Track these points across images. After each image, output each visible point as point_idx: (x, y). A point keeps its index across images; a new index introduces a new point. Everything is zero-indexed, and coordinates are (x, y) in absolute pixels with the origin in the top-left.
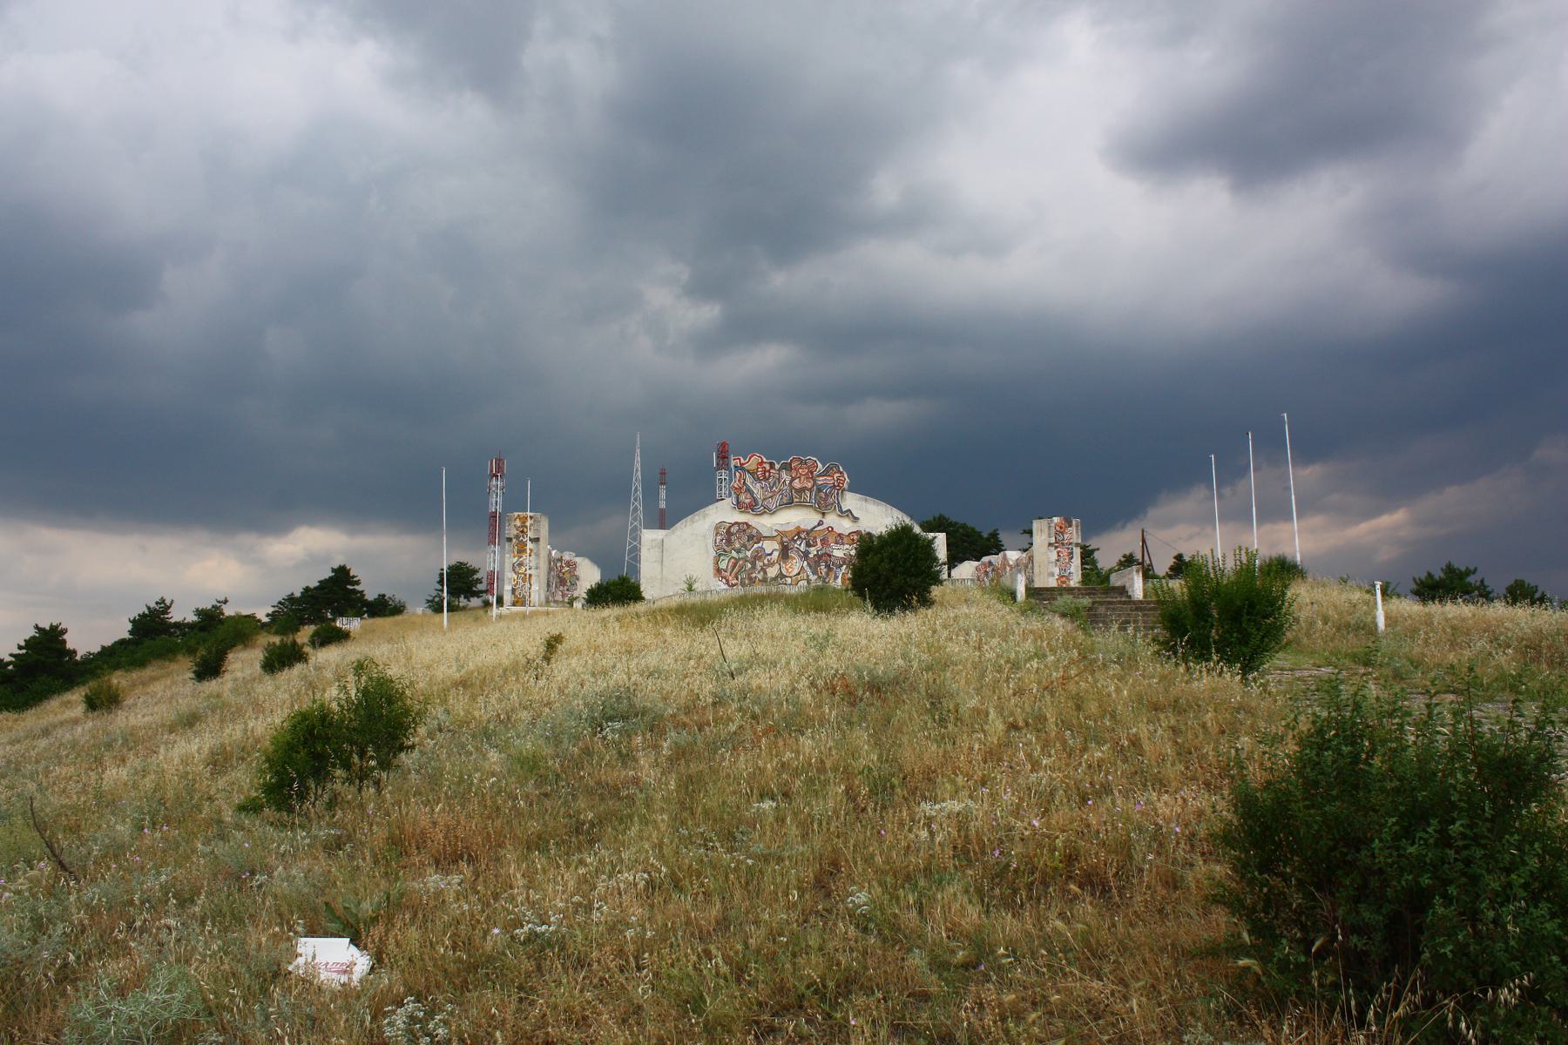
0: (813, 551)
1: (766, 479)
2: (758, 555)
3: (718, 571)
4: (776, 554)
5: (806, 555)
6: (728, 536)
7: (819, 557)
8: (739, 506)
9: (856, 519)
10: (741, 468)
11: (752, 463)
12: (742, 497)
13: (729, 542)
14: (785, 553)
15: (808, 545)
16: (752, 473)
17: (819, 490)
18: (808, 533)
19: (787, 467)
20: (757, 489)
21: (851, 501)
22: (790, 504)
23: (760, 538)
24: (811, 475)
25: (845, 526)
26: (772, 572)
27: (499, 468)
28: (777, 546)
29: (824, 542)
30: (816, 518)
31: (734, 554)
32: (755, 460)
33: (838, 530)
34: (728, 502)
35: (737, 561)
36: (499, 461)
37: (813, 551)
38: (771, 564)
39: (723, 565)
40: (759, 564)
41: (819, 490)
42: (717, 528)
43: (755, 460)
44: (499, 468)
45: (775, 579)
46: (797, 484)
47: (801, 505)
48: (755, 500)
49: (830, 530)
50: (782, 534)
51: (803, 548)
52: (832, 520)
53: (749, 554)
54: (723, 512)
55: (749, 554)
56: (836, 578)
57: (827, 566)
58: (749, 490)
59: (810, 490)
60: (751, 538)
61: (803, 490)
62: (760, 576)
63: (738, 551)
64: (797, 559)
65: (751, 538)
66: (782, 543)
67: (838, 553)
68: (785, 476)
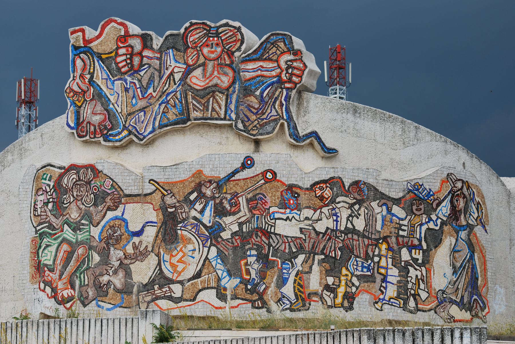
0: (230, 224)
1: (134, 71)
2: (112, 239)
3: (39, 268)
4: (151, 232)
5: (214, 234)
6: (64, 193)
7: (243, 237)
8: (81, 129)
9: (330, 153)
10: (85, 49)
11: (105, 39)
12: (87, 112)
13: (59, 208)
14: (170, 229)
15: (220, 212)
16: (107, 60)
17: (247, 91)
18: (220, 184)
19: (177, 44)
20: (115, 92)
21: (320, 114)
22: (182, 122)
23: (118, 198)
24: (228, 60)
25: (304, 167)
26: (143, 272)
27: (31, 91)
28: (153, 216)
29: (256, 202)
30: (244, 149)
31: (68, 233)
32: (113, 30)
33: (285, 177)
34: (59, 126)
35: (73, 246)
36: (30, 82)
37: (230, 224)
38: (140, 255)
39: (47, 258)
40: (116, 254)
41: (247, 91)
42: (37, 178)
43: (113, 30)
44: (31, 91)
45: (147, 287)
46: (197, 79)
47: (206, 124)
48: (110, 115)
49: (270, 176)
50: (163, 188)
51: (207, 218)
52: (275, 154)
53: (95, 232)
54: (52, 145)
55: (95, 232)
56: (282, 282)
57: (263, 258)
58: (100, 96)
59: (227, 92)
60: (99, 198)
61: (210, 91)
62: (118, 281)
63: (76, 228)
64: (195, 243)
65: (99, 198)
66: (163, 208)
67: (287, 228)
68: (174, 65)
